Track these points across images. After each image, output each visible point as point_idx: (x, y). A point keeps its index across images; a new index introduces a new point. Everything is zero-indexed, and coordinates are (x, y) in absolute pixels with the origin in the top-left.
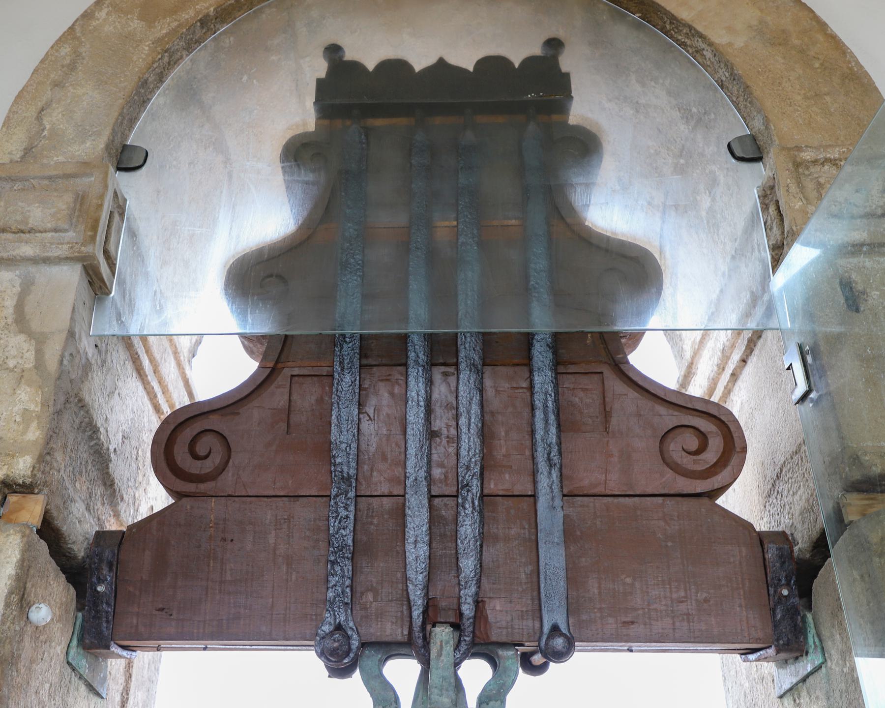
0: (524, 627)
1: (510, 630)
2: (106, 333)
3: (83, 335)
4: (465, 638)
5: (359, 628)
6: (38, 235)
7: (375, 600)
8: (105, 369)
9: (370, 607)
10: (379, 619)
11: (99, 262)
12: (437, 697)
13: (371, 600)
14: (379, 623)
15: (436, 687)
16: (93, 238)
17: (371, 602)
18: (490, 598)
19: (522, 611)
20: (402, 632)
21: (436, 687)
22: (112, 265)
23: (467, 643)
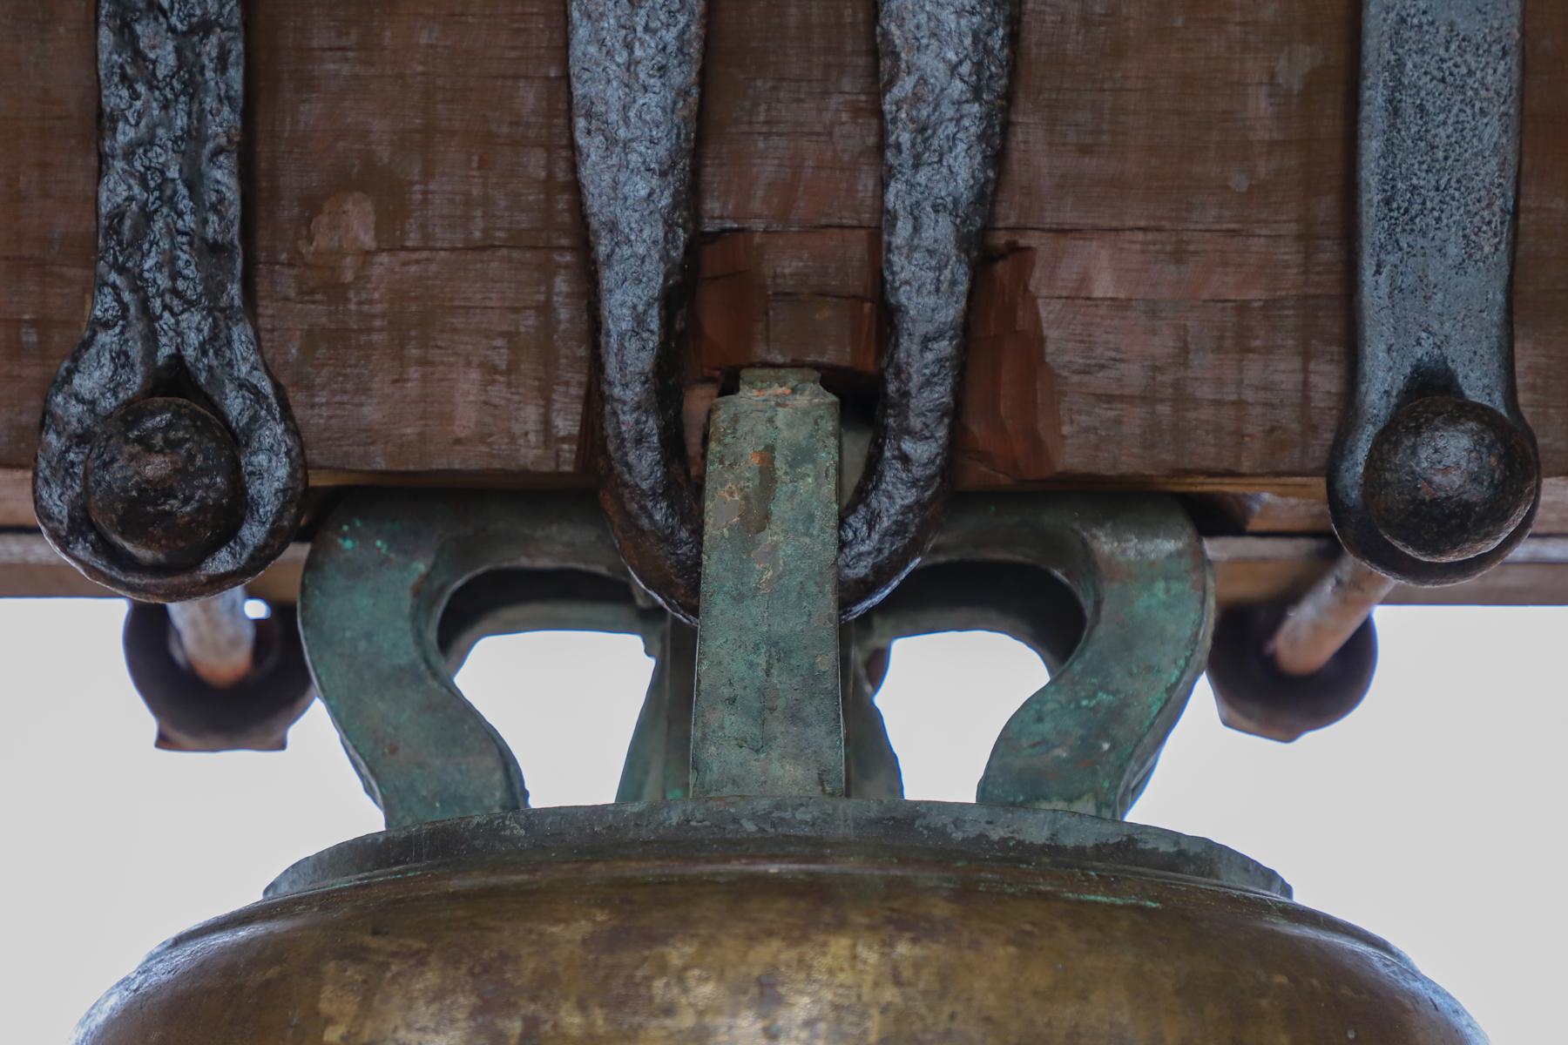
0: (1249, 395)
1: (1164, 409)
4: (908, 446)
5: (296, 397)
7: (389, 239)
9: (361, 278)
10: (414, 351)
12: (735, 755)
13: (367, 240)
14: (414, 373)
15: (732, 701)
17: (367, 255)
18: (1061, 231)
19: (1243, 308)
20: (546, 424)
21: (732, 701)
23: (917, 471)
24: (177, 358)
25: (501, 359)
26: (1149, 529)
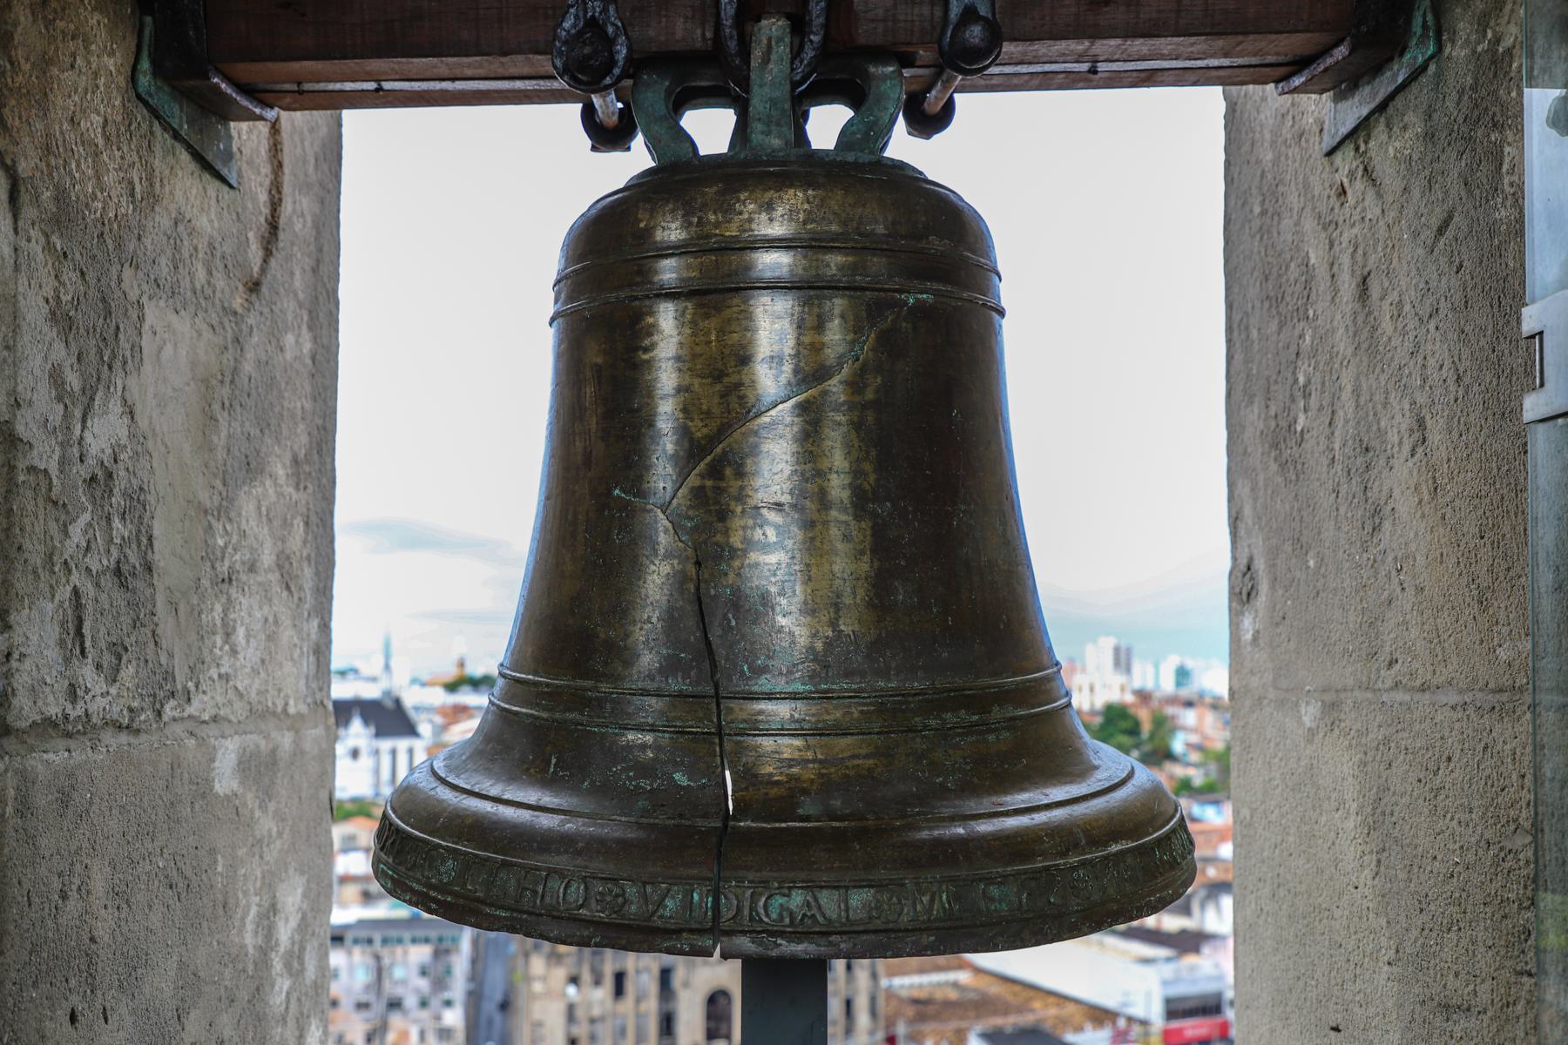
4: (812, 37)
5: (629, 28)
12: (761, 137)
15: (759, 120)
20: (703, 35)
21: (759, 120)
23: (815, 45)
24: (593, 16)
25: (689, 14)
26: (886, 64)
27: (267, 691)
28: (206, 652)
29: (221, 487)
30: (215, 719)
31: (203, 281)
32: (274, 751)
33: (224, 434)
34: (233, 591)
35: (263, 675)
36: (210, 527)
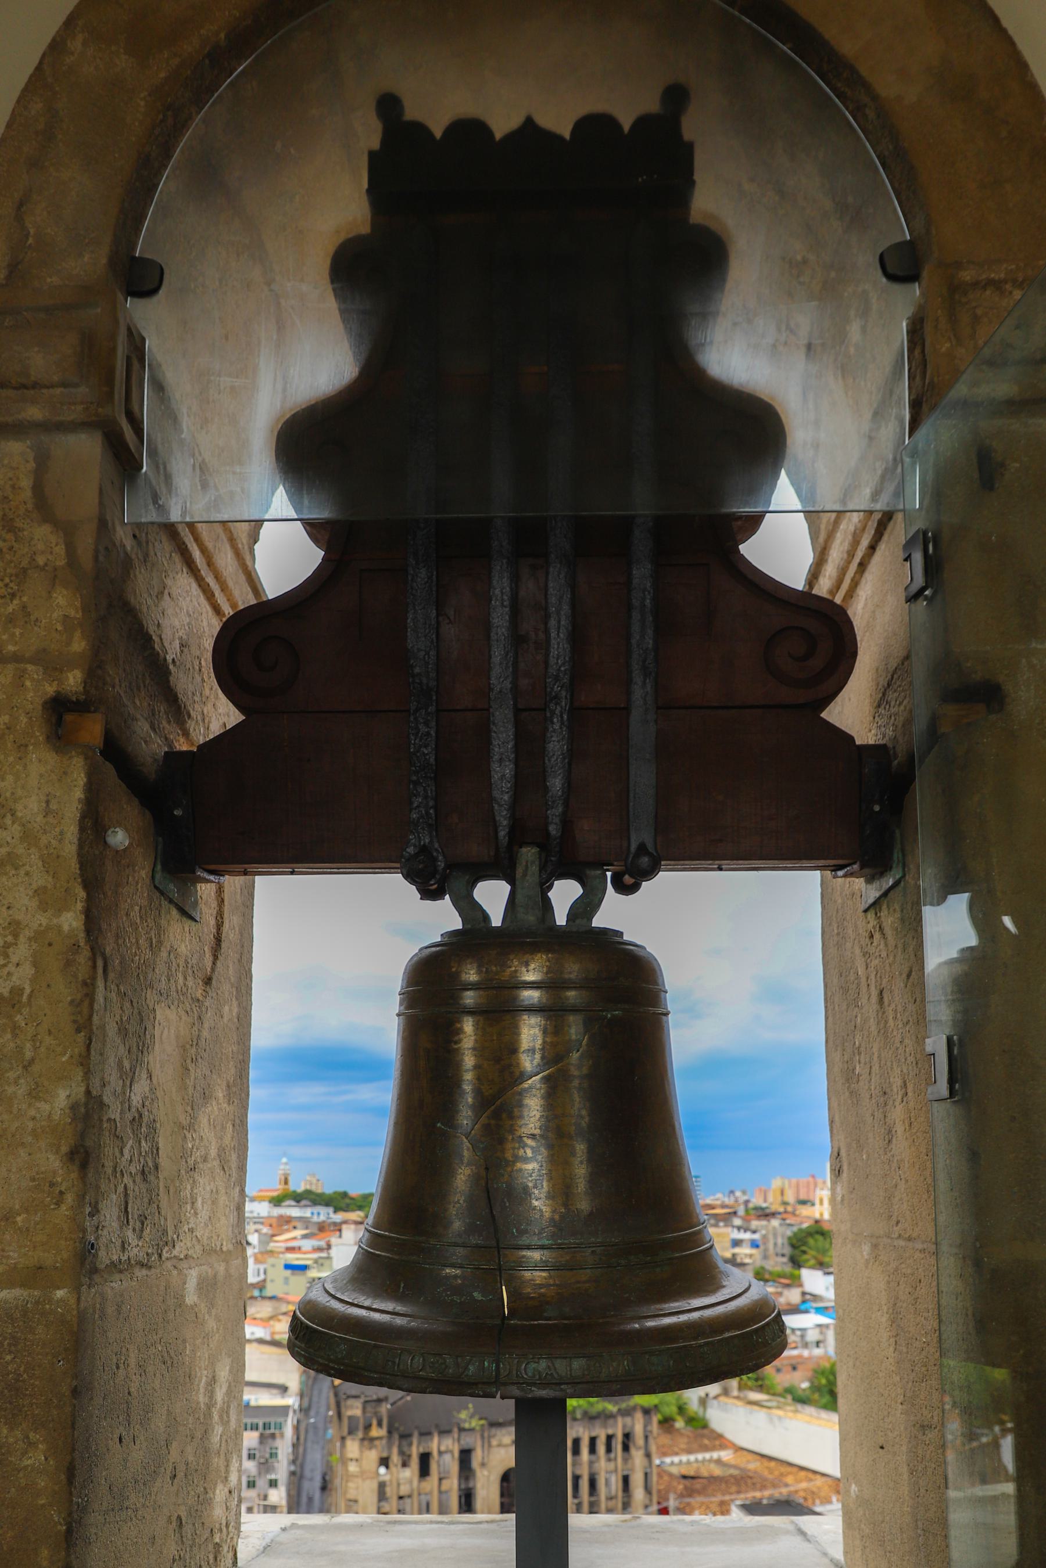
2: (143, 520)
3: (117, 523)
6: (45, 391)
8: (149, 564)
11: (122, 428)
16: (111, 394)
22: (138, 431)
27: (212, 1237)
28: (182, 1214)
29: (190, 1111)
30: (186, 1257)
31: (182, 984)
32: (215, 1276)
33: (192, 1078)
34: (196, 1175)
35: (210, 1227)
36: (185, 1137)
